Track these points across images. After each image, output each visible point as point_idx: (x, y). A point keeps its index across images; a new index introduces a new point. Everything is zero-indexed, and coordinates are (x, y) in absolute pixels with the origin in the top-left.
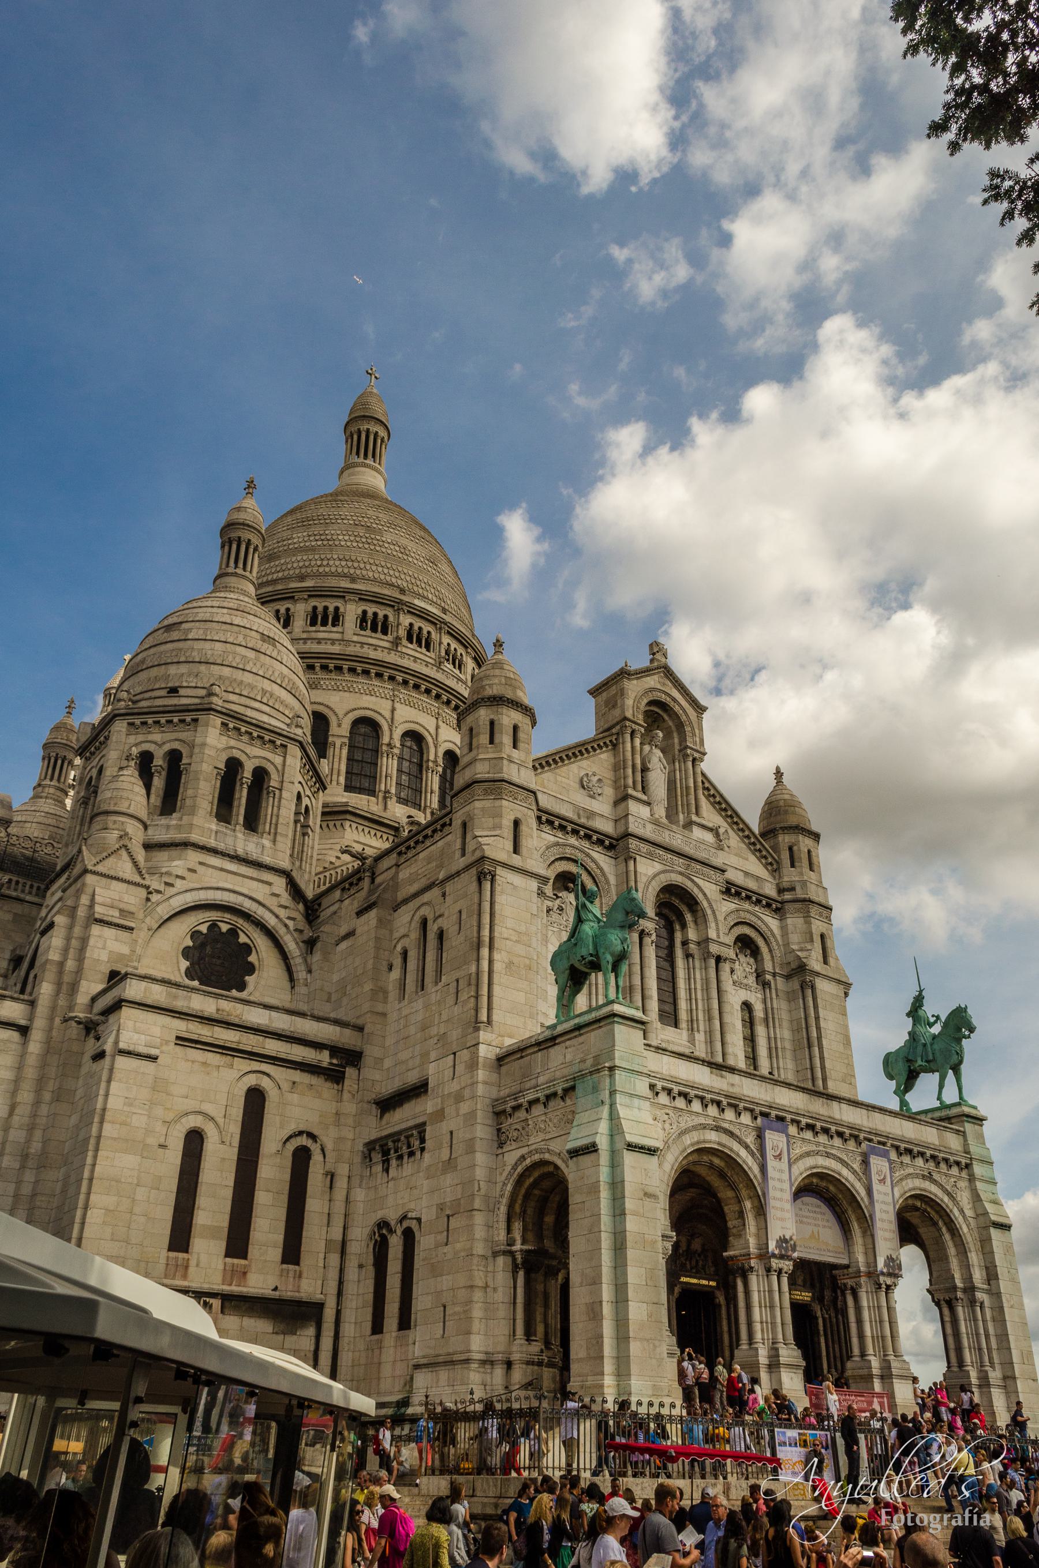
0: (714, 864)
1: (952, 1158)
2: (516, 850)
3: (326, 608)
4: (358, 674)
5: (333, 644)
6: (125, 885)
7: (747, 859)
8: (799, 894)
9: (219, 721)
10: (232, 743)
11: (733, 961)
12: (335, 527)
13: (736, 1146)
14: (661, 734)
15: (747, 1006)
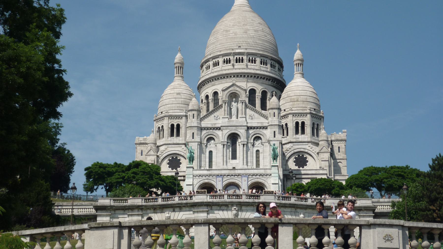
0: (243, 125)
1: (266, 174)
2: (193, 138)
3: (216, 61)
4: (223, 79)
5: (216, 73)
6: (152, 156)
7: (260, 119)
8: (270, 124)
9: (168, 118)
10: (171, 121)
11: (251, 143)
12: (219, 33)
13: (211, 181)
14: (234, 99)
15: (258, 151)
